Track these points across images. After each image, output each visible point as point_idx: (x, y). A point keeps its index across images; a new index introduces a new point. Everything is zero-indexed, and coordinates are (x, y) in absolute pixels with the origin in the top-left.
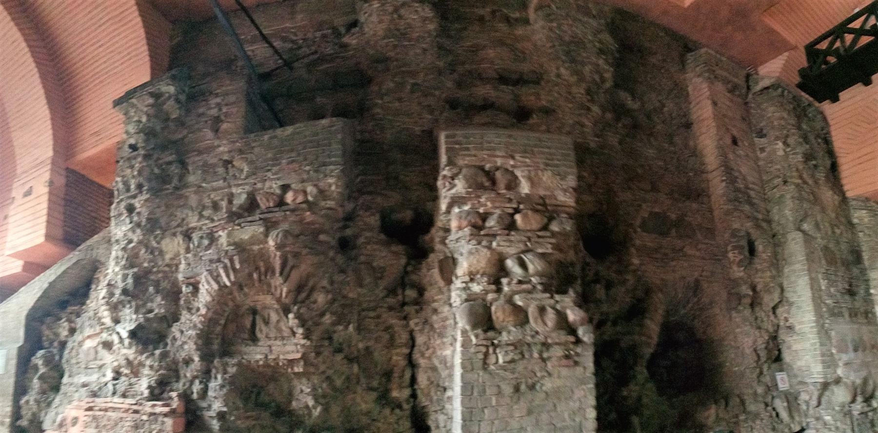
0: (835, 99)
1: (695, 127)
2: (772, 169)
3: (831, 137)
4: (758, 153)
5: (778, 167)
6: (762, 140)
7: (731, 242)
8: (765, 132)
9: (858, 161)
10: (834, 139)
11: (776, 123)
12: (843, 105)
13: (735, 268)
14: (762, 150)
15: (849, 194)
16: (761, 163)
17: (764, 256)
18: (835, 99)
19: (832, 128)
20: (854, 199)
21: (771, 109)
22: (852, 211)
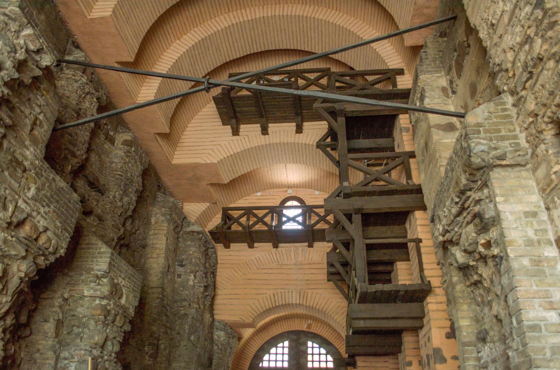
0: (227, 247)
1: (148, 250)
2: (182, 292)
3: (216, 272)
4: (176, 277)
5: (187, 292)
6: (181, 268)
7: (149, 340)
8: (184, 263)
9: (228, 297)
10: (218, 274)
11: (193, 260)
12: (231, 253)
13: (147, 357)
14: (179, 276)
15: (216, 317)
16: (176, 285)
17: (164, 353)
18: (227, 247)
19: (219, 266)
20: (218, 322)
21: (193, 249)
22: (215, 330)
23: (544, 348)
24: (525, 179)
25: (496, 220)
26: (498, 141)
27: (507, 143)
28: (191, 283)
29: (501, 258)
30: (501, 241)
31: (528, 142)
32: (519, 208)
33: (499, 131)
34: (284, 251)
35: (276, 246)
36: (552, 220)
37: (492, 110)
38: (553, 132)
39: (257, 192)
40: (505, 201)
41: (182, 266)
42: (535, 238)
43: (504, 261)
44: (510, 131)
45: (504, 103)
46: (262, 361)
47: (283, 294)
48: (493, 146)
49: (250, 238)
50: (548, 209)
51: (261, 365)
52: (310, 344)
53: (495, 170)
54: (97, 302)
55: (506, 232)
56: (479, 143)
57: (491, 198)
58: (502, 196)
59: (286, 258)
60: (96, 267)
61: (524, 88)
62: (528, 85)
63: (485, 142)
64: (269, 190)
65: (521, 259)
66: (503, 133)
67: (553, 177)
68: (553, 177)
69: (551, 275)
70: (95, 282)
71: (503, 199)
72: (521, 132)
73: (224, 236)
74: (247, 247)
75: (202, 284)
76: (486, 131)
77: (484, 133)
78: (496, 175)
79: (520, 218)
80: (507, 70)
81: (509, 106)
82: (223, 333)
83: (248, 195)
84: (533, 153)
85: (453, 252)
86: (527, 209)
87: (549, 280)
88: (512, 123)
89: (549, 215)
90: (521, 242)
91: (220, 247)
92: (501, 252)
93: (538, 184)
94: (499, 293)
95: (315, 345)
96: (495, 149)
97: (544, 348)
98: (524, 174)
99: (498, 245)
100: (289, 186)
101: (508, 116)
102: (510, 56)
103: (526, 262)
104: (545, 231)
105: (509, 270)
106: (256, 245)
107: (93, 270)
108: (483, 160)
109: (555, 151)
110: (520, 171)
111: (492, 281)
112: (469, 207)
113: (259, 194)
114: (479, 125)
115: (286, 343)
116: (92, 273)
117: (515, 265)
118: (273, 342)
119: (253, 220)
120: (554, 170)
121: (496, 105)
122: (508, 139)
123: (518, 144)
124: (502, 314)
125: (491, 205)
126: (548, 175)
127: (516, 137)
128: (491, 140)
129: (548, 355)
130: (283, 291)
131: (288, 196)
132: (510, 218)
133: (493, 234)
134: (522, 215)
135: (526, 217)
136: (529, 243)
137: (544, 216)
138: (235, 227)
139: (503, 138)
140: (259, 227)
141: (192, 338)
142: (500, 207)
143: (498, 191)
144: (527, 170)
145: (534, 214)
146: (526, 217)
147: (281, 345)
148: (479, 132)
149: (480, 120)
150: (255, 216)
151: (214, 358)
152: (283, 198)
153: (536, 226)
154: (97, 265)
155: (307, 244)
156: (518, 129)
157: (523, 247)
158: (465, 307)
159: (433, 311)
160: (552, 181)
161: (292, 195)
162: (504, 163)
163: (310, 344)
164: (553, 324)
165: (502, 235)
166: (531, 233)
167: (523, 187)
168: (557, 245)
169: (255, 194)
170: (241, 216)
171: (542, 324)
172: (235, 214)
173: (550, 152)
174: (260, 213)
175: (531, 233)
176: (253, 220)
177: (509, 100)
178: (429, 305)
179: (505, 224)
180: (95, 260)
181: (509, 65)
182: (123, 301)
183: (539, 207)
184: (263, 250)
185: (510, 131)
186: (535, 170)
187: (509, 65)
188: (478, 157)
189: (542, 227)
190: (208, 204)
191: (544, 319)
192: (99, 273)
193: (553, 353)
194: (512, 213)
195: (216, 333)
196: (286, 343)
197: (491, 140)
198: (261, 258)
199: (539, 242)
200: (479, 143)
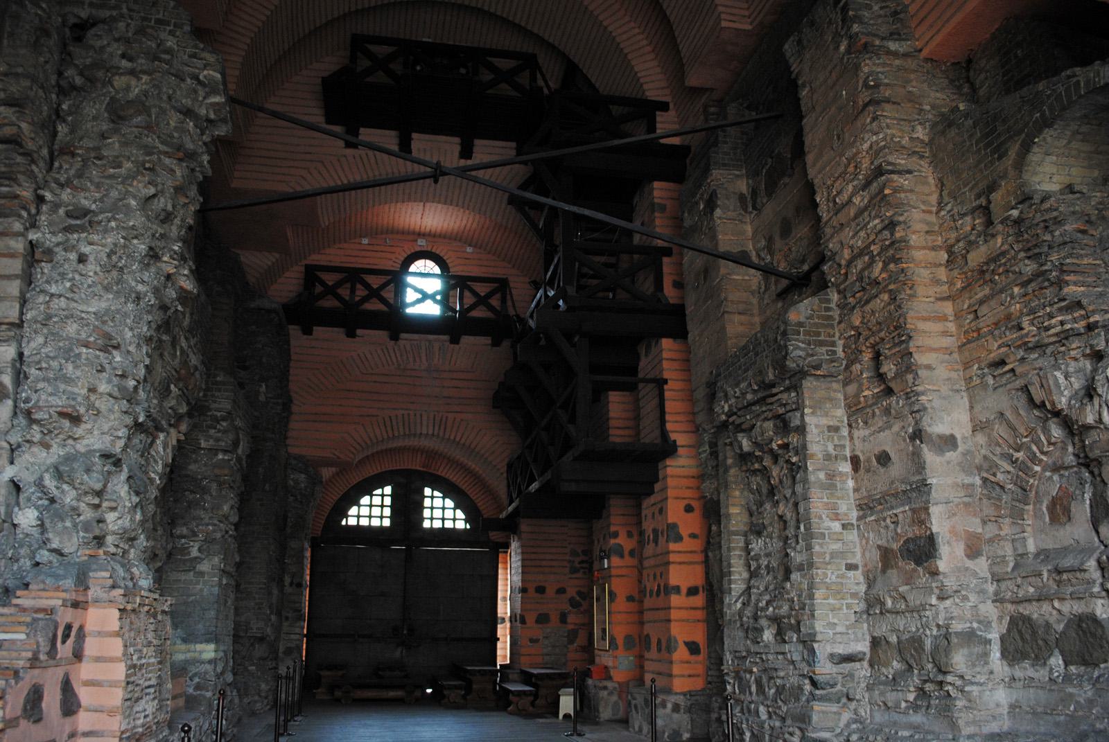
0: (308, 331)
11: (264, 360)
18: (308, 331)
20: (295, 458)
23: (825, 553)
24: (835, 391)
25: (802, 430)
26: (816, 345)
27: (824, 349)
28: (262, 398)
29: (799, 467)
30: (802, 450)
31: (844, 351)
32: (825, 421)
33: (819, 334)
34: (408, 348)
35: (395, 337)
36: (852, 438)
37: (815, 308)
38: (870, 356)
39: (361, 237)
40: (812, 413)
41: (245, 368)
42: (834, 453)
43: (801, 471)
44: (829, 335)
45: (829, 301)
46: (347, 516)
47: (406, 416)
48: (810, 352)
49: (352, 320)
50: (850, 426)
51: (344, 523)
52: (428, 491)
53: (808, 378)
54: (220, 457)
55: (809, 446)
56: (798, 348)
57: (799, 407)
58: (811, 408)
59: (411, 360)
60: (214, 406)
61: (853, 296)
62: (858, 295)
63: (803, 345)
64: (384, 236)
65: (818, 472)
66: (822, 338)
67: (862, 399)
68: (862, 399)
69: (841, 489)
70: (215, 428)
71: (811, 410)
72: (840, 338)
73: (303, 314)
74: (343, 336)
75: (280, 401)
76: (807, 333)
77: (804, 335)
78: (808, 384)
79: (823, 432)
80: (840, 265)
81: (833, 305)
82: (303, 476)
83: (345, 242)
84: (847, 367)
85: (740, 439)
86: (831, 424)
87: (839, 494)
88: (832, 326)
89: (850, 432)
90: (820, 456)
91: (294, 331)
92: (800, 461)
93: (845, 399)
94: (788, 496)
95: (436, 493)
96: (812, 355)
97: (825, 553)
98: (835, 385)
99: (797, 454)
100: (421, 235)
101: (830, 318)
102: (847, 254)
103: (822, 475)
104: (843, 447)
105: (805, 481)
106: (359, 332)
107: (210, 410)
108: (798, 366)
109: (870, 375)
110: (831, 382)
111: (781, 482)
112: (772, 404)
113: (365, 241)
114: (800, 324)
115: (388, 490)
116: (209, 413)
117: (812, 478)
118: (367, 487)
119: (361, 292)
120: (864, 394)
121: (821, 301)
122: (826, 345)
123: (834, 352)
124: (789, 515)
125: (798, 414)
126: (857, 395)
127: (833, 344)
128: (809, 344)
129: (827, 559)
130: (406, 412)
131: (418, 249)
132: (815, 431)
133: (794, 439)
134: (826, 429)
135: (829, 431)
136: (828, 457)
137: (845, 432)
138: (329, 303)
139: (822, 343)
140: (374, 306)
141: (267, 487)
142: (807, 419)
143: (807, 403)
144: (838, 382)
145: (836, 429)
146: (829, 431)
147: (379, 491)
148: (799, 333)
149: (802, 319)
150: (367, 286)
151: (290, 515)
152: (409, 253)
153: (836, 442)
154: (215, 402)
155: (446, 337)
156: (837, 335)
157: (821, 461)
158: (737, 493)
159: (672, 476)
160: (860, 403)
161: (425, 249)
162: (819, 372)
163: (428, 491)
164: (835, 533)
165: (804, 447)
166: (830, 448)
167: (831, 400)
168: (852, 462)
169: (357, 241)
170: (339, 284)
171: (826, 532)
172: (330, 279)
173: (864, 376)
174: (375, 281)
175: (830, 448)
176: (361, 292)
177: (835, 297)
178: (668, 469)
179: (809, 438)
180: (209, 393)
181: (843, 262)
182: (240, 451)
183: (843, 422)
184: (371, 341)
185: (829, 335)
186: (846, 383)
187: (843, 262)
188: (794, 362)
189: (842, 443)
190: (277, 256)
191: (829, 528)
192: (219, 414)
193: (832, 558)
194: (817, 426)
195: (292, 476)
196: (388, 490)
197: (809, 344)
198: (369, 356)
199: (836, 457)
200: (798, 348)
